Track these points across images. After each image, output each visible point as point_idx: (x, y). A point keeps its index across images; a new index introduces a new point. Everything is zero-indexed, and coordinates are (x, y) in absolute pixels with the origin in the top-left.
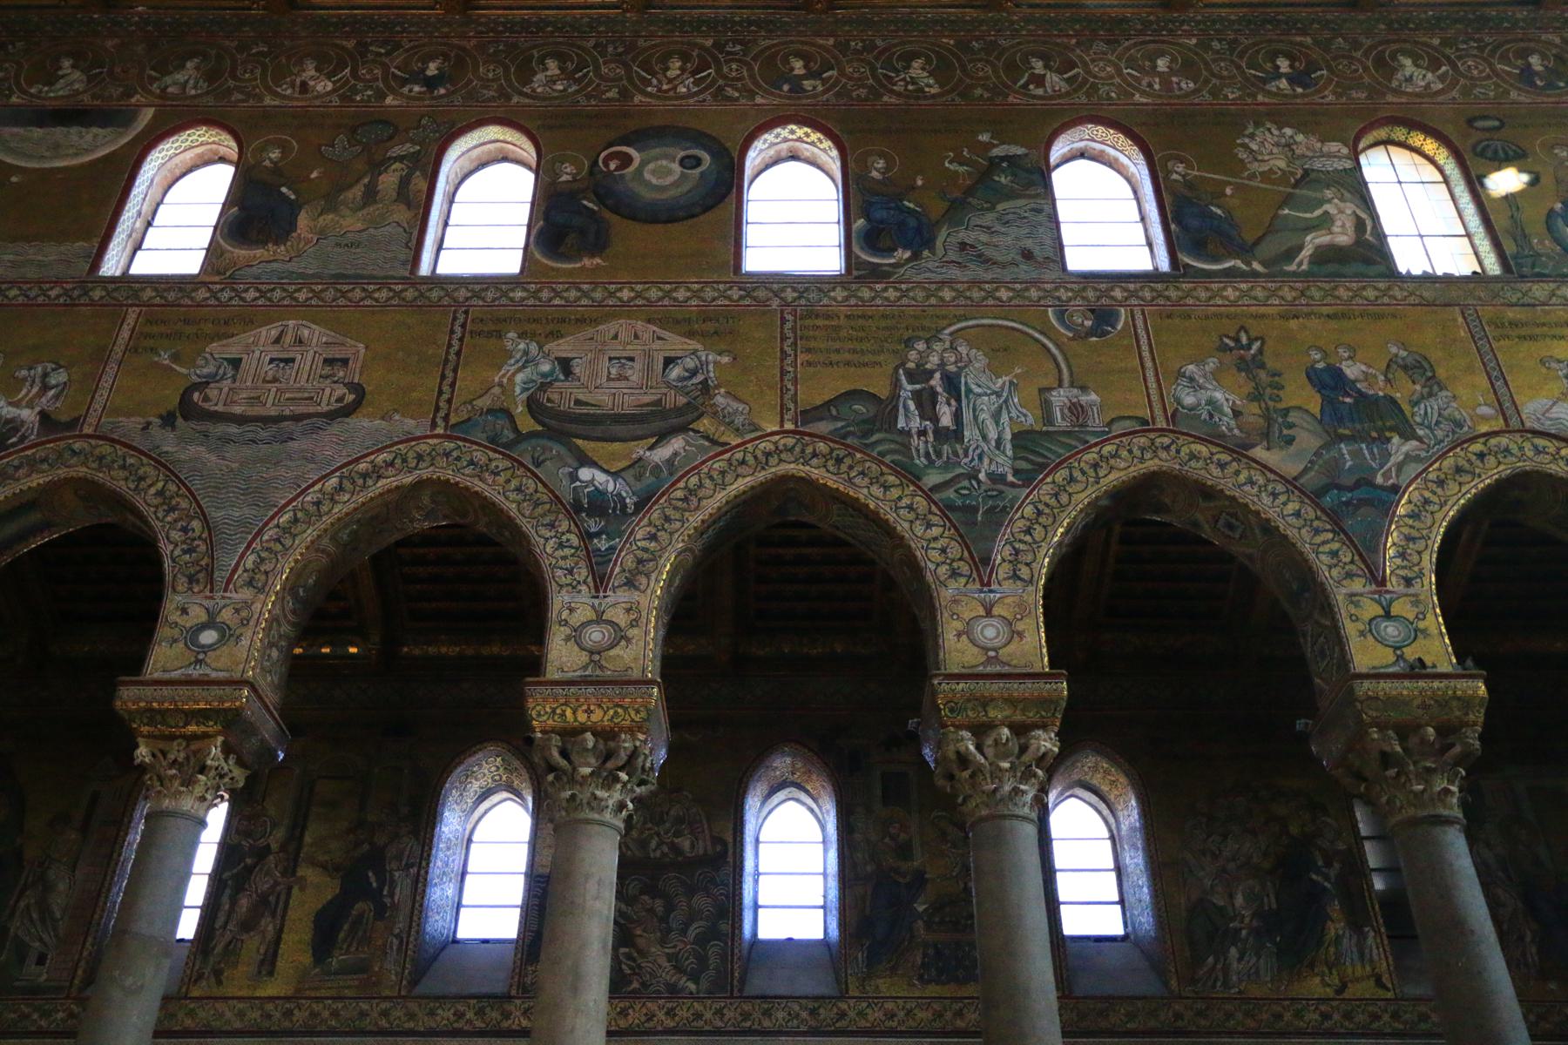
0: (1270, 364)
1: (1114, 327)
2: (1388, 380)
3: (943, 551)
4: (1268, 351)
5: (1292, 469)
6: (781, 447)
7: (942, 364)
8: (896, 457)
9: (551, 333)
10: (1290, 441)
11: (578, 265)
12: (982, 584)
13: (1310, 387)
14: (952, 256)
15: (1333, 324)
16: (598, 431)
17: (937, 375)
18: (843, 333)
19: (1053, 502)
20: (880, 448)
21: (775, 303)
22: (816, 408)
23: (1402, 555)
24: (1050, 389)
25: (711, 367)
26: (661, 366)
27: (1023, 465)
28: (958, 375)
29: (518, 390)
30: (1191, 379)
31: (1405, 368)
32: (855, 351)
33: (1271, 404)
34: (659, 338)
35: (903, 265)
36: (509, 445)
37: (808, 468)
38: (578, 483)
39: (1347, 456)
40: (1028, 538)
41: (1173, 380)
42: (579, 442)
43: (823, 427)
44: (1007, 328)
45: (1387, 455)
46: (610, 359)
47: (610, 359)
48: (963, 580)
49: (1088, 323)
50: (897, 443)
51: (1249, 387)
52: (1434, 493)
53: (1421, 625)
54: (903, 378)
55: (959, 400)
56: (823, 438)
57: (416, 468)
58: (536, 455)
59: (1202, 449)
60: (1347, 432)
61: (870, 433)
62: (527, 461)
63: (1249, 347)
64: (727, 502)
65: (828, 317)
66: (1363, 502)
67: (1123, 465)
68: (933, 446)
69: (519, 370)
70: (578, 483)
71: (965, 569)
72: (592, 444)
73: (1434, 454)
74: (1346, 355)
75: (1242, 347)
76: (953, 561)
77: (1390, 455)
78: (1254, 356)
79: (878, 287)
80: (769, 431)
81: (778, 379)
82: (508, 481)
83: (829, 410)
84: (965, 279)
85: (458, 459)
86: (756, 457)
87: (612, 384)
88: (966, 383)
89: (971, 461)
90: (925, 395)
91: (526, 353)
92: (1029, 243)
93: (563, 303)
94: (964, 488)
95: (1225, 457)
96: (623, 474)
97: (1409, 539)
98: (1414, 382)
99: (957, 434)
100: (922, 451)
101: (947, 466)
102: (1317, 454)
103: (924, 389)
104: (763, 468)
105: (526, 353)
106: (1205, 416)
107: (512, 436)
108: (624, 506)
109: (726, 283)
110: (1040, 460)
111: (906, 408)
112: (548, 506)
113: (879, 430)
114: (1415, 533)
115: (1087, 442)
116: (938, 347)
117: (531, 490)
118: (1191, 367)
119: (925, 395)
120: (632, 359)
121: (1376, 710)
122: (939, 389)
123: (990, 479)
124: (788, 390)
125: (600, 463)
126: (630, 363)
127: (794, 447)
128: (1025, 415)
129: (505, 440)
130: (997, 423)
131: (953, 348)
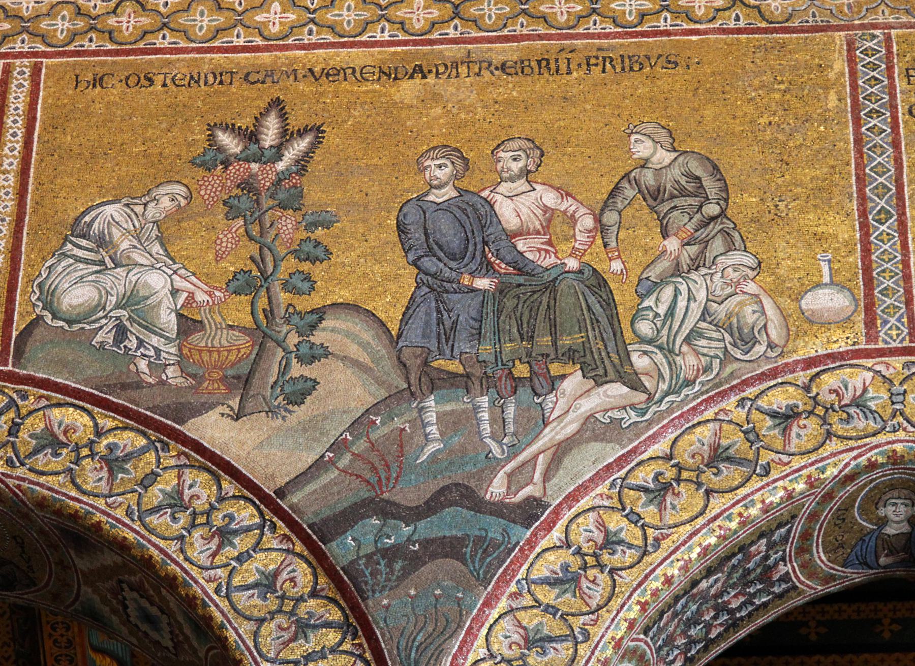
30: (102, 242)
33: (283, 297)
39: (433, 430)
41: (55, 242)
60: (454, 366)
63: (278, 151)
73: (660, 416)
74: (516, 167)
77: (545, 425)
95: (131, 440)
106: (105, 336)
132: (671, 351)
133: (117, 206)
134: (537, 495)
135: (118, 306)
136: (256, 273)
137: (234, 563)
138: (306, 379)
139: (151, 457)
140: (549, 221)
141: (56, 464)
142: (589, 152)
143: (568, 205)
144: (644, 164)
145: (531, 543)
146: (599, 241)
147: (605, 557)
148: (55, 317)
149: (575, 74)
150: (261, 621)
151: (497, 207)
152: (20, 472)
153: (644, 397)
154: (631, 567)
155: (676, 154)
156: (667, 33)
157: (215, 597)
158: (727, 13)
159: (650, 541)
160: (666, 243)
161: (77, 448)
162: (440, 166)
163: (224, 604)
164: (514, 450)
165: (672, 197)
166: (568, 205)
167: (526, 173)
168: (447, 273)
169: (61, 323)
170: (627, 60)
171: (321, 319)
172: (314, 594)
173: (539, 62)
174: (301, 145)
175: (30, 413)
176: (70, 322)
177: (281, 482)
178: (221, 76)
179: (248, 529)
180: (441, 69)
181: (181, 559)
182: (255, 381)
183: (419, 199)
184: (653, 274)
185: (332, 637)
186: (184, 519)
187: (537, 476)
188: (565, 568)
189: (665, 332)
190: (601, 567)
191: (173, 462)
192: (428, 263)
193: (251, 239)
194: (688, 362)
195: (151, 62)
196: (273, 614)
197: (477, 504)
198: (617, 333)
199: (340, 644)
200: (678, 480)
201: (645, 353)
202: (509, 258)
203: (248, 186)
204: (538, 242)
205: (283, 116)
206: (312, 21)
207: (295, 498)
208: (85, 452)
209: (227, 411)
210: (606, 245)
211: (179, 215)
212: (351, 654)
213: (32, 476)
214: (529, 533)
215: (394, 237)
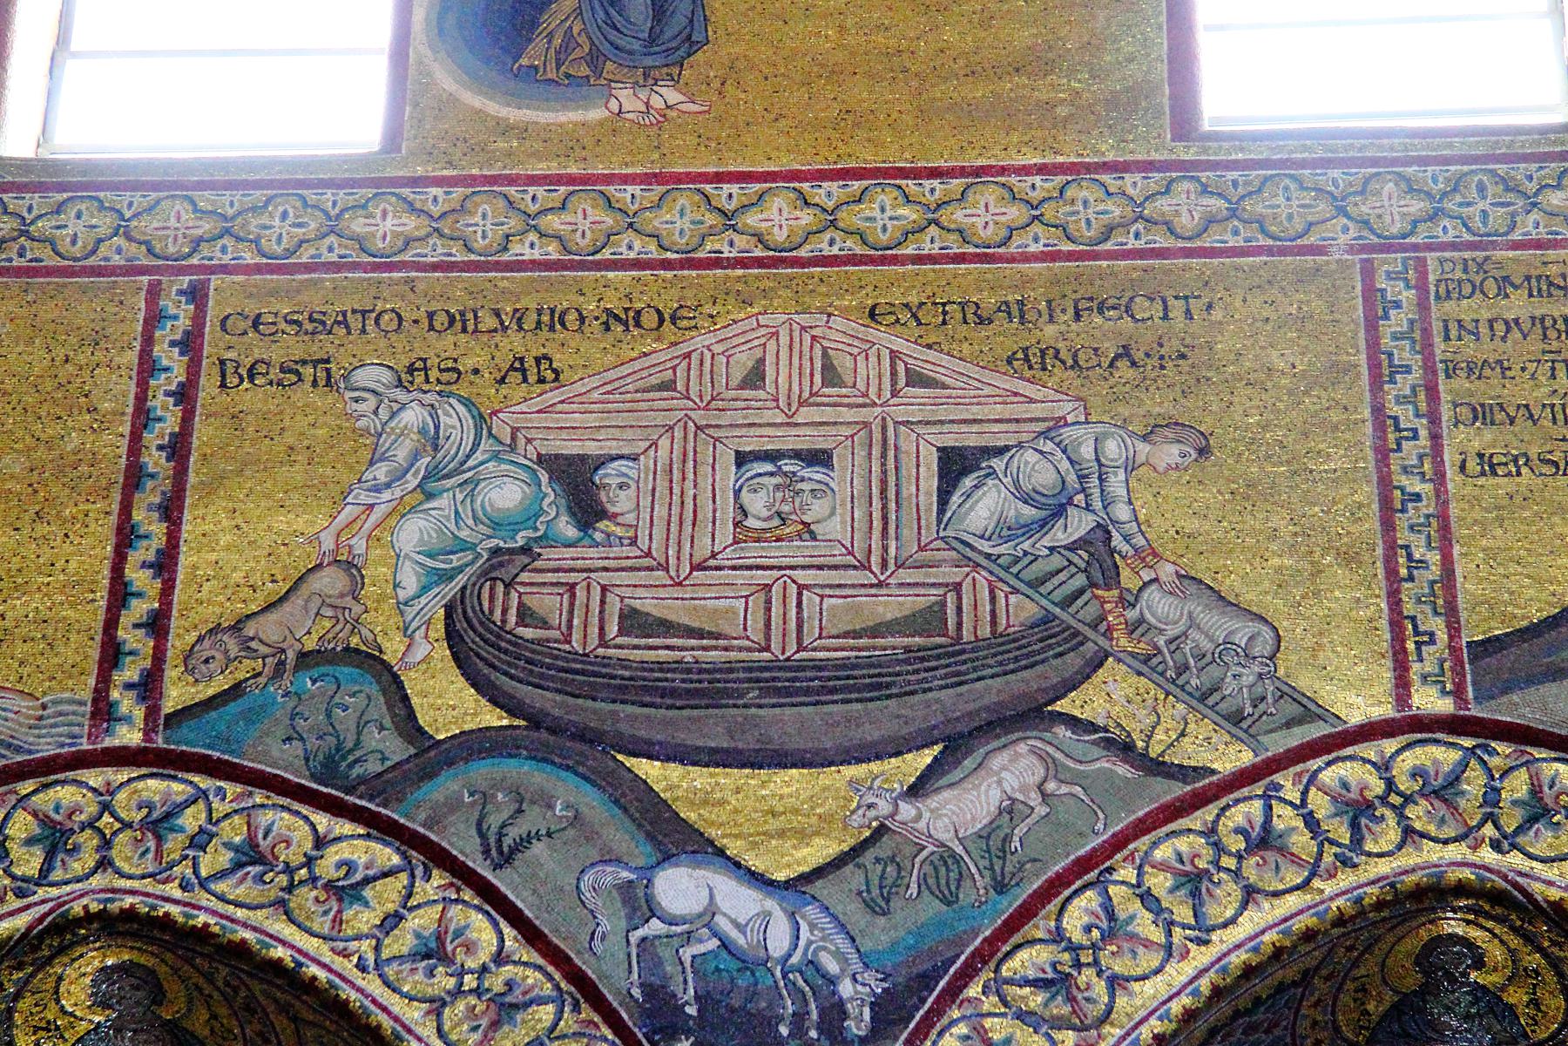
6: (1404, 784)
9: (519, 365)
11: (596, 114)
16: (713, 730)
21: (1341, 234)
25: (1116, 483)
26: (931, 483)
29: (410, 581)
34: (915, 379)
36: (388, 784)
37: (1516, 859)
38: (655, 927)
42: (649, 769)
46: (742, 459)
47: (742, 459)
57: (43, 878)
58: (494, 821)
62: (465, 848)
64: (1217, 992)
69: (400, 511)
70: (655, 927)
72: (700, 778)
80: (1355, 719)
81: (1373, 524)
82: (392, 921)
85: (200, 841)
86: (1311, 822)
87: (753, 552)
91: (433, 440)
93: (553, 251)
96: (818, 887)
104: (1346, 862)
105: (433, 440)
107: (397, 749)
108: (835, 1012)
109: (1148, 167)
112: (546, 1013)
117: (484, 956)
120: (819, 458)
124: (1416, 564)
125: (734, 848)
126: (816, 473)
127: (1455, 779)
129: (374, 767)
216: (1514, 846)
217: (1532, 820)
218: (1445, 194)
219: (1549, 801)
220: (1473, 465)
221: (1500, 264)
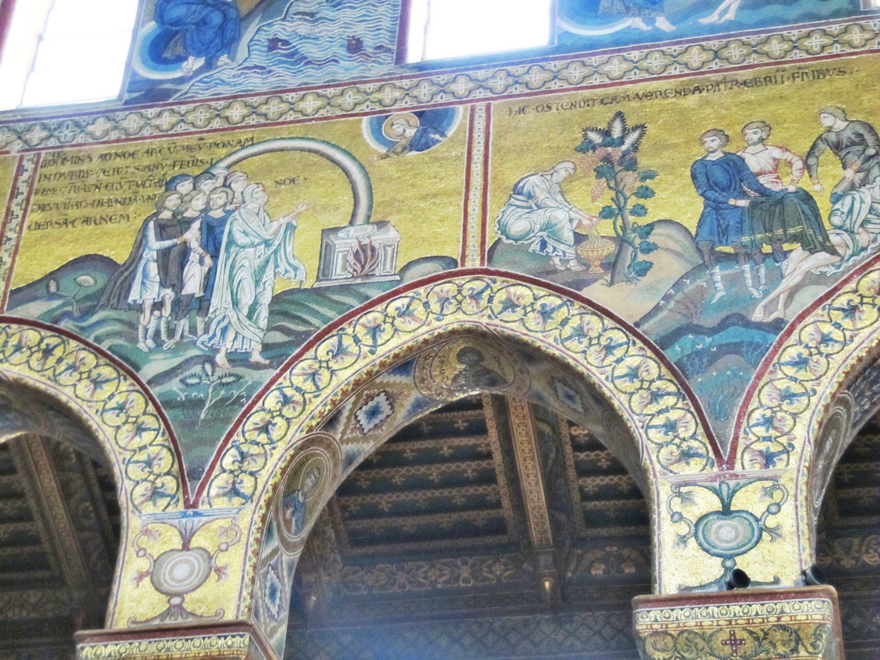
0: (644, 162)
1: (443, 134)
2: (807, 167)
3: (149, 463)
4: (645, 145)
5: (631, 311)
7: (206, 210)
8: (120, 341)
10: (643, 270)
12: (187, 505)
13: (693, 189)
14: (258, 59)
15: (749, 95)
17: (196, 225)
18: (92, 180)
19: (309, 386)
20: (100, 331)
21: (18, 145)
22: (35, 283)
23: (768, 422)
24: (336, 230)
27: (278, 337)
28: (222, 222)
30: (530, 196)
31: (837, 147)
32: (100, 203)
33: (631, 219)
35: (191, 78)
39: (720, 285)
40: (263, 438)
41: (505, 199)
43: (34, 310)
44: (302, 150)
45: (778, 276)
48: (163, 502)
49: (411, 132)
50: (120, 321)
51: (606, 199)
52: (838, 326)
53: (771, 522)
54: (151, 233)
55: (215, 257)
56: (34, 324)
59: (524, 292)
60: (728, 249)
61: (91, 311)
63: (622, 141)
65: (78, 160)
66: (735, 348)
67: (414, 325)
68: (168, 323)
71: (170, 484)
73: (849, 268)
74: (756, 138)
75: (612, 144)
76: (159, 476)
77: (782, 277)
78: (624, 155)
79: (151, 112)
83: (48, 287)
84: (265, 89)
88: (230, 232)
89: (210, 339)
90: (174, 253)
92: (359, 30)
94: (193, 376)
95: (554, 301)
97: (788, 396)
98: (845, 167)
99: (202, 304)
100: (151, 332)
101: (180, 346)
102: (678, 285)
103: (175, 245)
106: (536, 247)
110: (301, 328)
111: (145, 275)
113: (104, 307)
114: (796, 388)
115: (367, 298)
116: (206, 185)
118: (534, 179)
119: (174, 253)
121: (663, 651)
122: (194, 244)
123: (230, 361)
128: (296, 269)
130: (257, 283)
131: (226, 185)
132: (852, 232)
133: (536, 176)
134: (781, 316)
135: (541, 230)
136: (614, 206)
137: (614, 364)
138: (646, 262)
139: (564, 309)
140: (777, 166)
141: (514, 317)
142: (797, 125)
143: (788, 156)
144: (830, 130)
145: (780, 343)
146: (806, 174)
147: (822, 348)
148: (507, 238)
149: (786, 83)
150: (632, 394)
151: (746, 161)
152: (496, 321)
153: (838, 258)
154: (838, 353)
155: (847, 123)
156: (838, 56)
157: (606, 382)
158: (872, 41)
159: (848, 338)
160: (845, 172)
161: (525, 308)
162: (712, 141)
163: (611, 386)
164: (766, 293)
165: (847, 147)
166: (788, 156)
167: (761, 140)
168: (721, 199)
169: (511, 241)
170: (816, 74)
171: (652, 229)
172: (660, 378)
173: (765, 78)
174: (635, 135)
175: (499, 290)
176: (516, 240)
177: (637, 319)
178: (588, 102)
179: (621, 345)
180: (710, 87)
181: (585, 363)
182: (619, 265)
183: (702, 159)
184: (839, 191)
185: (671, 400)
186: (585, 341)
187: (781, 305)
188: (799, 355)
189: (848, 222)
190: (820, 353)
191: (576, 312)
192: (709, 194)
193: (610, 188)
194: (863, 238)
195: (549, 98)
196: (638, 390)
197: (748, 324)
198: (821, 226)
199: (676, 404)
200: (862, 303)
201: (837, 234)
202: (755, 187)
203: (607, 159)
204: (771, 177)
205: (623, 121)
206: (636, 67)
207: (645, 326)
208: (529, 309)
209: (605, 282)
210: (811, 176)
211: (570, 179)
212: (683, 409)
213: (503, 324)
214: (778, 338)
215: (690, 181)
216: (7, 361)
217: (15, 351)
218: (55, 129)
219: (23, 344)
220: (33, 227)
221: (65, 153)
